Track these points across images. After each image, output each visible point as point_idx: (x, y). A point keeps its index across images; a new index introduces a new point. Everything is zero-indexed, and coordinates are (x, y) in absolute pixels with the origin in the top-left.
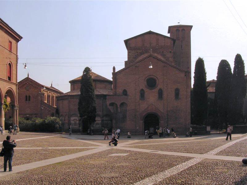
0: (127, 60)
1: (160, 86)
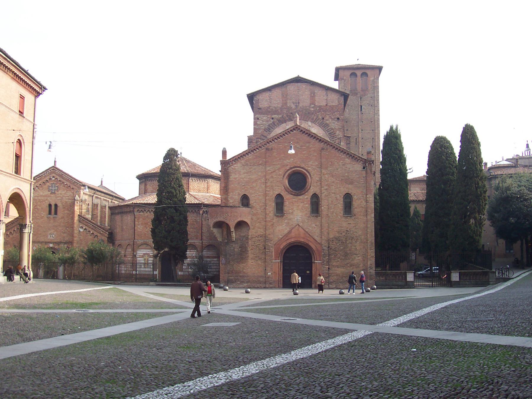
0: (252, 134)
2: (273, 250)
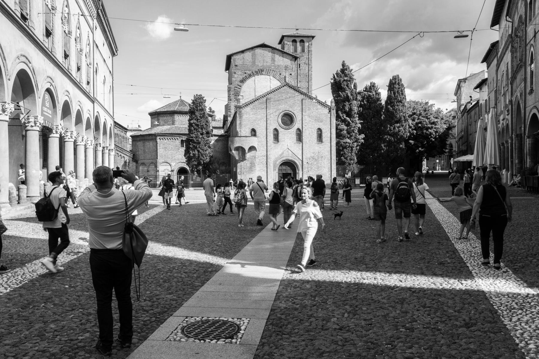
1: (297, 125)
2: (272, 165)
